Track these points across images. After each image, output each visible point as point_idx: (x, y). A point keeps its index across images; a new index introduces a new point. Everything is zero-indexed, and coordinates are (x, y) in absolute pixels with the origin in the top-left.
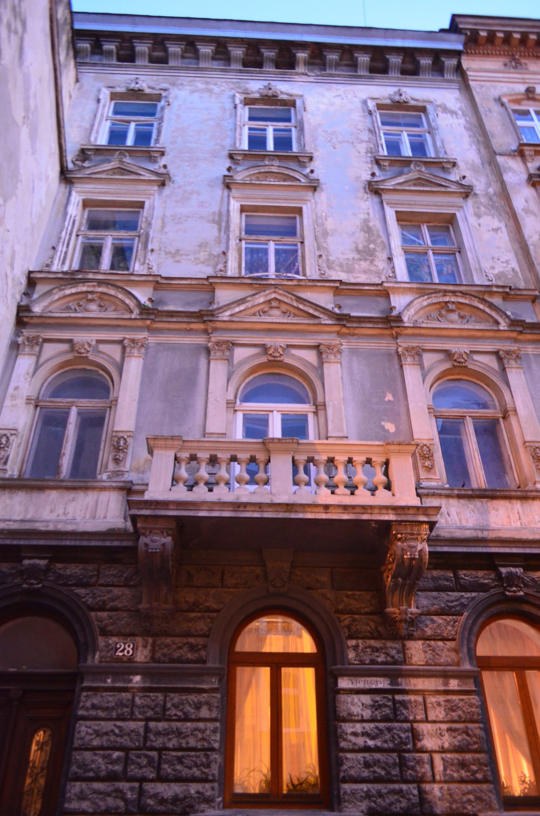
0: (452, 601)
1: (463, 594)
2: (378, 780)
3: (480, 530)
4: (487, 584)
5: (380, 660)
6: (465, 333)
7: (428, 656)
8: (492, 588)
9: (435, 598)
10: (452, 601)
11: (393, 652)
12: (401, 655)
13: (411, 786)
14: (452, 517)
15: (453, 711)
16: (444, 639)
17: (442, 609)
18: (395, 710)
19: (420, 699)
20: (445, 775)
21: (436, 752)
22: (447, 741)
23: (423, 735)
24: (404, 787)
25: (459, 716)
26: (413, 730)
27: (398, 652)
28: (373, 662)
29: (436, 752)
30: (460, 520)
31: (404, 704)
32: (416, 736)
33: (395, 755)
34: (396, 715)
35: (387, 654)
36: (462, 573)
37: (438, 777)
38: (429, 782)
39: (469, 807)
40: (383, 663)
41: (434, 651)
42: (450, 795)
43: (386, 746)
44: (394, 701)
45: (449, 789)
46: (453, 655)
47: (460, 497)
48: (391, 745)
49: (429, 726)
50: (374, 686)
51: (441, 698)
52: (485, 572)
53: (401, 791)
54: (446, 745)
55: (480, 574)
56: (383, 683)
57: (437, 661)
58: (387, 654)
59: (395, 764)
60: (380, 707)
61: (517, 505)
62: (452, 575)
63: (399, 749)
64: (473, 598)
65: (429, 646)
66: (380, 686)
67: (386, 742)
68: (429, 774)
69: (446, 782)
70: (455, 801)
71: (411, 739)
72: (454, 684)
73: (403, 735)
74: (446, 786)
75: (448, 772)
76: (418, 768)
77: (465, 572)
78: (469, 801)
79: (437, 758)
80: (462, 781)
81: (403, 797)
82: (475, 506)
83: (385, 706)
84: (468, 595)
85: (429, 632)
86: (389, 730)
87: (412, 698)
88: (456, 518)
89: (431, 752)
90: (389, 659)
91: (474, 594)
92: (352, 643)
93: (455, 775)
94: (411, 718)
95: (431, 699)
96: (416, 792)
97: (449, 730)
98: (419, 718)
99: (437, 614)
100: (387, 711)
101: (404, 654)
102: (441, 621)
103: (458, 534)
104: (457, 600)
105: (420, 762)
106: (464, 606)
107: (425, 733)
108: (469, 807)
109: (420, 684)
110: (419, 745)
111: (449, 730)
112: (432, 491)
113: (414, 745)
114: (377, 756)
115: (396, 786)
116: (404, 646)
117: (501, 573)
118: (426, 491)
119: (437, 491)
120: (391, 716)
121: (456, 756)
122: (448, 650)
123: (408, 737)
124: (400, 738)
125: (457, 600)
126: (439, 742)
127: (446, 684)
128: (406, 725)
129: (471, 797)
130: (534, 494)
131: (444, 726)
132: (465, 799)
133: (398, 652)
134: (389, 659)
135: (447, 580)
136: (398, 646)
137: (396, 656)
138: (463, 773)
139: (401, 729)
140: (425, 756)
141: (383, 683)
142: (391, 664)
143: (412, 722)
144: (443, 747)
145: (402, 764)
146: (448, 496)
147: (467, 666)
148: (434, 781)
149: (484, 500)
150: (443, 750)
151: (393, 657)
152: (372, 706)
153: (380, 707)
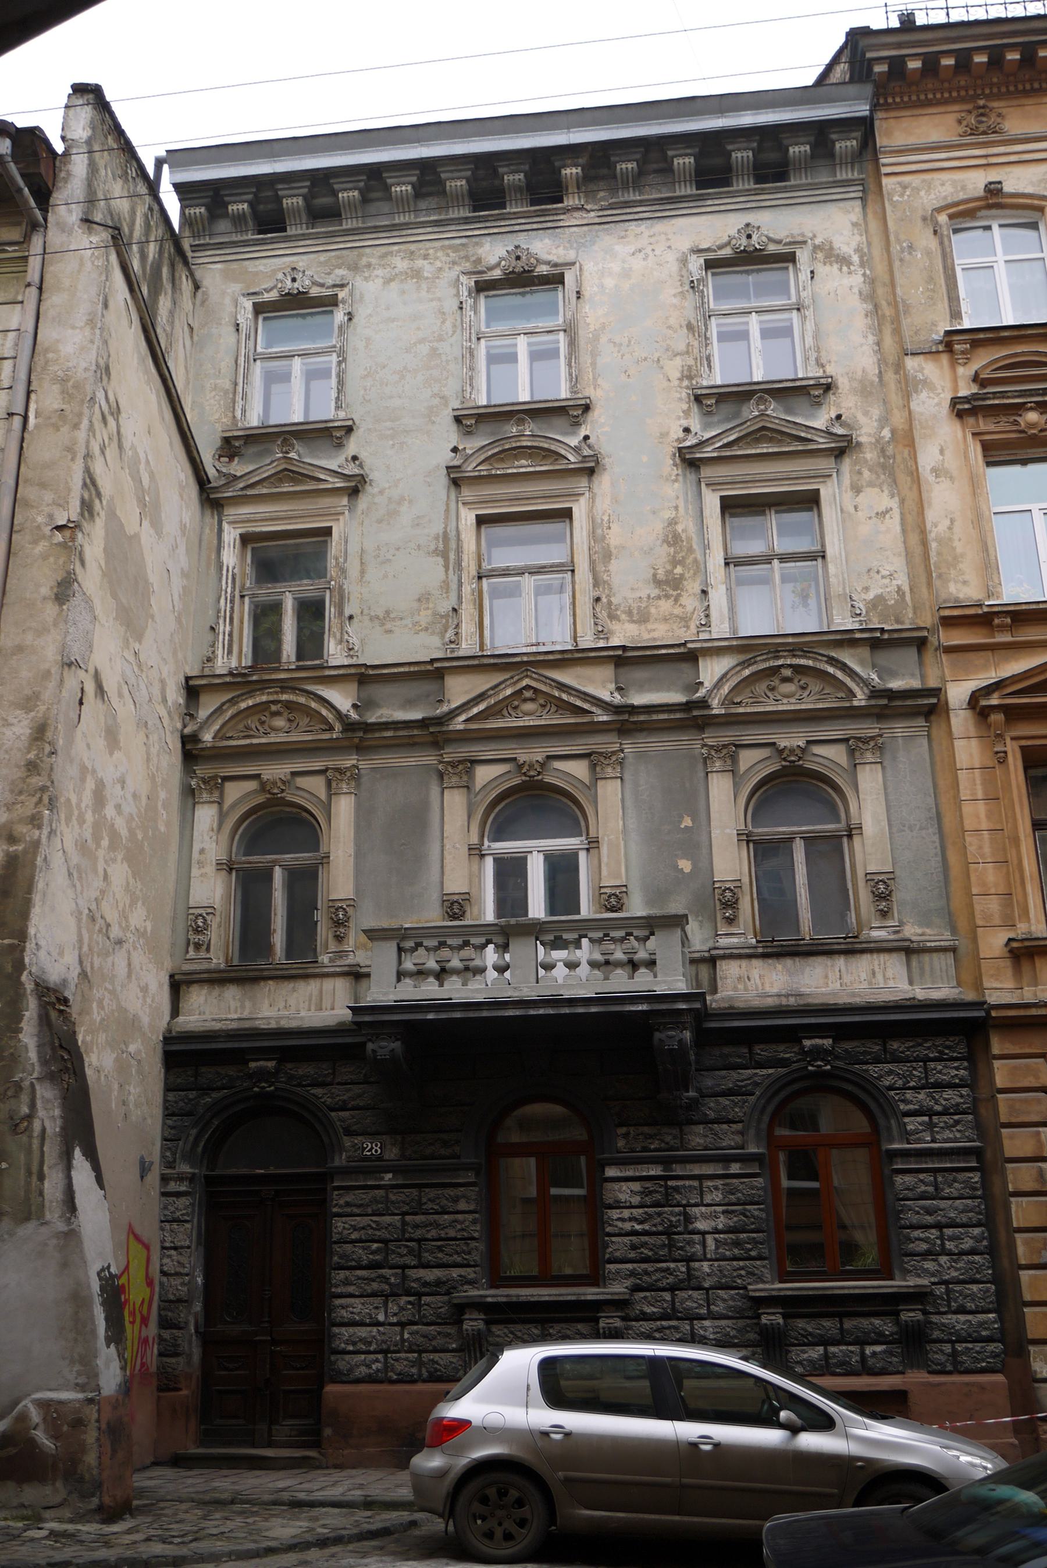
0: (742, 1081)
1: (758, 1071)
2: (646, 1260)
3: (785, 996)
4: (788, 1059)
5: (652, 1147)
6: (802, 715)
7: (708, 1140)
8: (794, 1062)
9: (724, 1078)
10: (742, 1081)
11: (668, 1138)
12: (678, 1141)
13: (679, 1264)
14: (752, 982)
15: (733, 1194)
16: (729, 1122)
17: (729, 1089)
18: (667, 1194)
19: (696, 1183)
20: (716, 1253)
21: (709, 1233)
22: (721, 1222)
23: (696, 1218)
24: (672, 1265)
25: (738, 1199)
26: (685, 1214)
27: (675, 1137)
28: (645, 1149)
29: (709, 1233)
30: (763, 984)
31: (676, 1189)
32: (688, 1219)
33: (663, 1237)
34: (668, 1200)
35: (662, 1141)
36: (757, 1049)
37: (709, 1256)
38: (701, 1260)
39: (739, 1281)
40: (655, 1150)
41: (716, 1135)
42: (720, 1271)
43: (654, 1229)
44: (666, 1187)
45: (719, 1266)
46: (738, 1139)
47: (765, 956)
48: (660, 1228)
49: (703, 1209)
50: (644, 1174)
51: (719, 1183)
52: (787, 1045)
53: (668, 1269)
54: (720, 1226)
55: (782, 1047)
56: (655, 1171)
57: (717, 1145)
58: (662, 1141)
59: (664, 1245)
60: (651, 1192)
61: (841, 962)
62: (746, 1050)
63: (668, 1233)
64: (769, 1075)
65: (711, 1129)
66: (652, 1173)
67: (655, 1225)
68: (700, 1253)
69: (716, 1260)
70: (725, 1276)
71: (682, 1222)
72: (735, 1168)
73: (674, 1219)
74: (716, 1264)
75: (720, 1250)
76: (688, 1248)
77: (762, 1046)
78: (740, 1276)
79: (710, 1240)
80: (735, 1259)
81: (671, 1274)
82: (784, 967)
83: (657, 1192)
84: (765, 1072)
85: (712, 1115)
86: (659, 1214)
87: (687, 1183)
88: (758, 981)
89: (703, 1233)
90: (663, 1145)
91: (771, 1071)
92: (623, 1130)
93: (728, 1253)
94: (684, 1202)
95: (710, 1183)
96: (684, 1269)
97: (724, 1212)
98: (692, 1202)
99: (724, 1094)
100: (658, 1196)
101: (682, 1139)
102: (727, 1103)
103: (757, 1003)
104: (749, 1079)
105: (691, 1243)
106: (757, 1084)
107: (698, 1215)
108: (739, 1281)
109: (697, 1170)
110: (691, 1227)
111: (724, 1212)
112: (728, 951)
113: (686, 1227)
114: (646, 1238)
115: (664, 1265)
116: (681, 1131)
117: (804, 1047)
118: (721, 952)
119: (735, 951)
120: (663, 1201)
121: (730, 1236)
122: (733, 1133)
123: (679, 1220)
124: (671, 1221)
125: (749, 1079)
126: (713, 1224)
127: (727, 1168)
128: (677, 1209)
129: (743, 1272)
130: (864, 945)
131: (719, 1209)
132: (735, 1274)
133: (675, 1137)
134: (663, 1145)
135: (739, 1057)
136: (676, 1131)
137: (672, 1143)
138: (736, 1251)
139: (672, 1213)
140: (696, 1237)
141: (655, 1171)
142: (664, 1151)
143: (684, 1206)
144: (716, 1229)
145: (671, 1245)
146: (750, 956)
147: (752, 1149)
148: (707, 1260)
149: (797, 959)
150: (716, 1231)
151: (667, 1143)
152: (642, 1193)
153: (651, 1192)
